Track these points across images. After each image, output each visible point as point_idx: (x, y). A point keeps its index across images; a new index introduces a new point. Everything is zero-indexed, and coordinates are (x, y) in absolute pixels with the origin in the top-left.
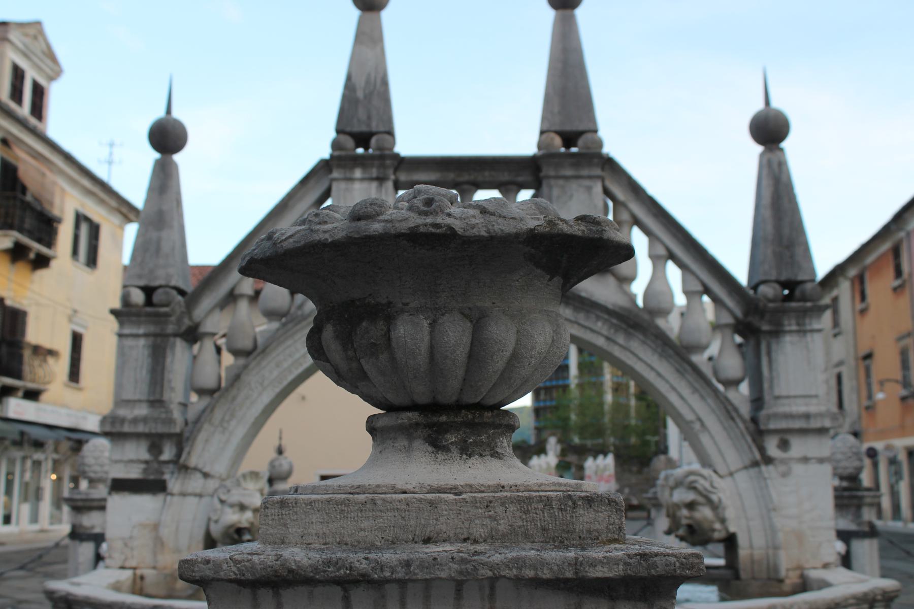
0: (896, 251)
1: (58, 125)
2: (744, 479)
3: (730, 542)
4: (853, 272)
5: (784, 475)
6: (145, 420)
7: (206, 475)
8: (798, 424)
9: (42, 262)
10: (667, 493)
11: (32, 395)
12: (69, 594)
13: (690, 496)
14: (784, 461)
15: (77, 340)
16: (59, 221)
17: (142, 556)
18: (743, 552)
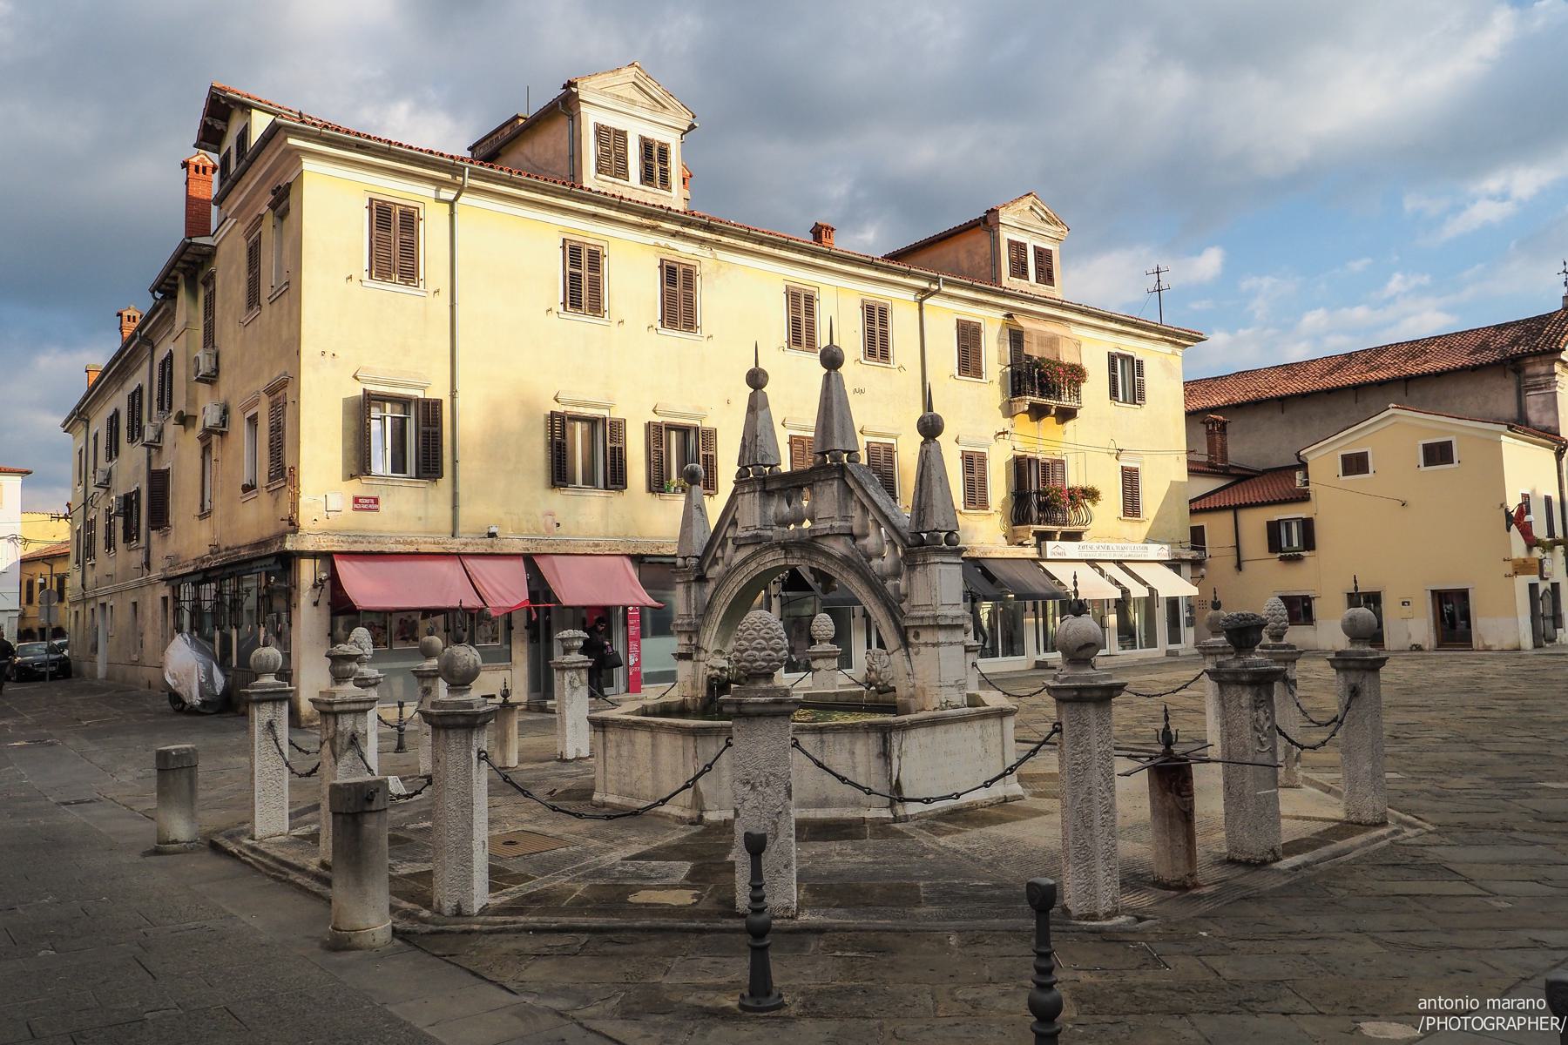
11: (1075, 536)
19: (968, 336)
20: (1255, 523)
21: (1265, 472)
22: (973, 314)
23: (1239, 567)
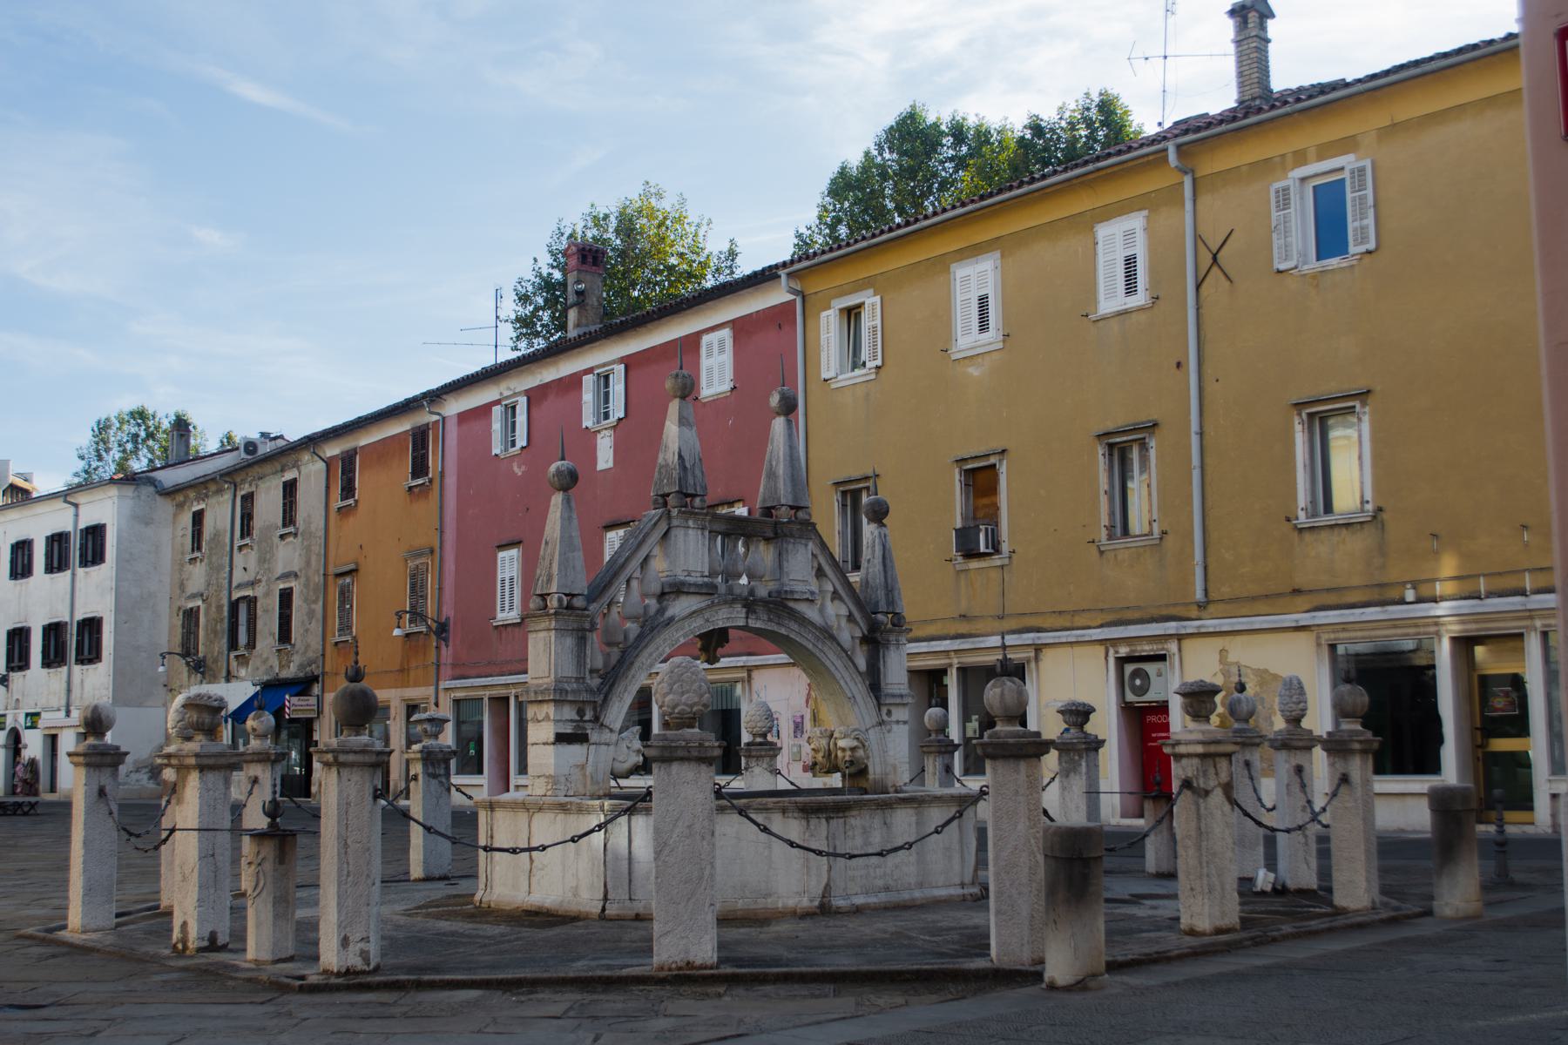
4: (333, 450)
8: (898, 701)
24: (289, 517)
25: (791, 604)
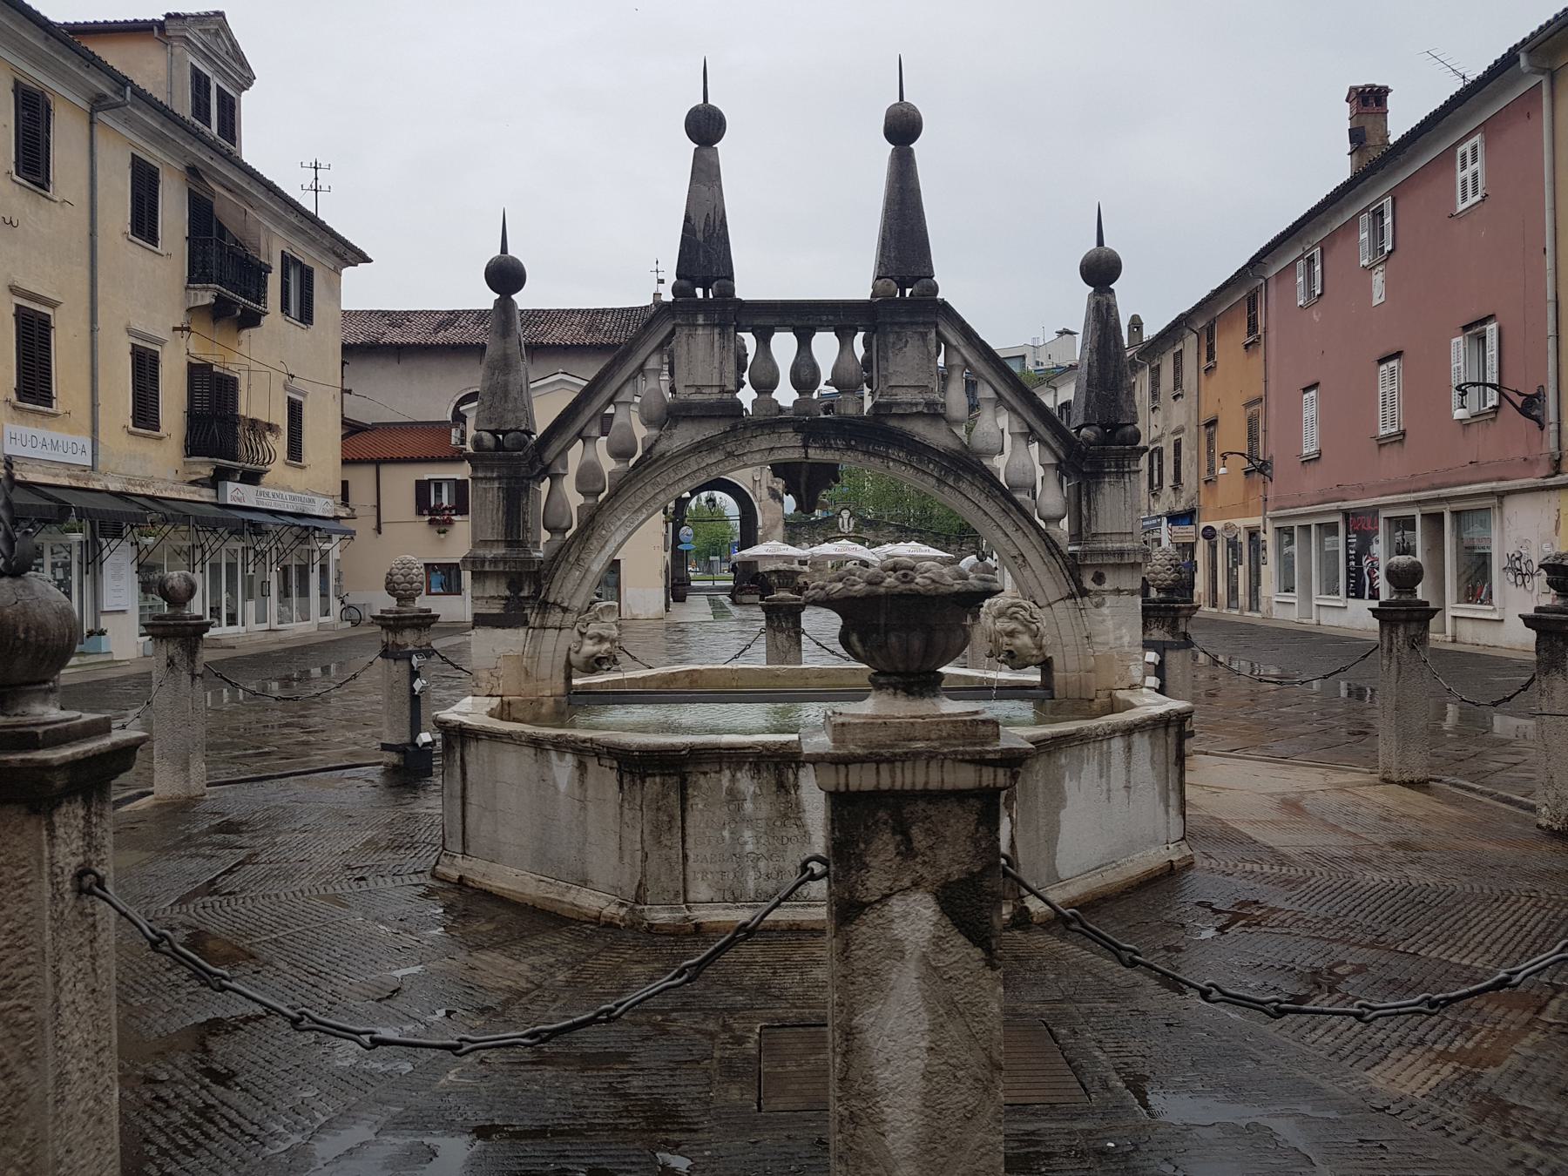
0: (1252, 302)
1: (257, 148)
2: (1063, 610)
3: (1046, 666)
5: (1098, 606)
6: (504, 560)
7: (565, 610)
9: (252, 319)
10: (990, 620)
11: (252, 478)
12: (461, 724)
13: (1013, 625)
14: (1097, 593)
15: (295, 410)
16: (269, 269)
17: (511, 686)
18: (1057, 676)
19: (144, 182)
20: (400, 483)
21: (375, 427)
22: (155, 155)
23: (379, 530)
24: (1178, 383)
25: (893, 423)
